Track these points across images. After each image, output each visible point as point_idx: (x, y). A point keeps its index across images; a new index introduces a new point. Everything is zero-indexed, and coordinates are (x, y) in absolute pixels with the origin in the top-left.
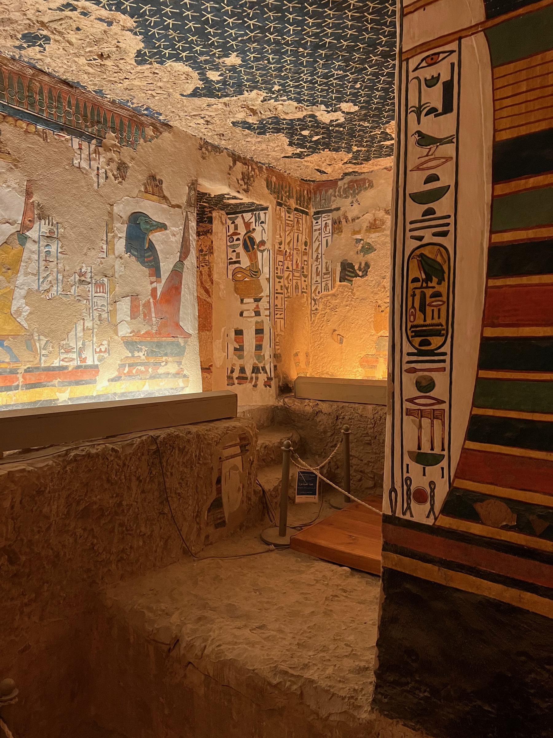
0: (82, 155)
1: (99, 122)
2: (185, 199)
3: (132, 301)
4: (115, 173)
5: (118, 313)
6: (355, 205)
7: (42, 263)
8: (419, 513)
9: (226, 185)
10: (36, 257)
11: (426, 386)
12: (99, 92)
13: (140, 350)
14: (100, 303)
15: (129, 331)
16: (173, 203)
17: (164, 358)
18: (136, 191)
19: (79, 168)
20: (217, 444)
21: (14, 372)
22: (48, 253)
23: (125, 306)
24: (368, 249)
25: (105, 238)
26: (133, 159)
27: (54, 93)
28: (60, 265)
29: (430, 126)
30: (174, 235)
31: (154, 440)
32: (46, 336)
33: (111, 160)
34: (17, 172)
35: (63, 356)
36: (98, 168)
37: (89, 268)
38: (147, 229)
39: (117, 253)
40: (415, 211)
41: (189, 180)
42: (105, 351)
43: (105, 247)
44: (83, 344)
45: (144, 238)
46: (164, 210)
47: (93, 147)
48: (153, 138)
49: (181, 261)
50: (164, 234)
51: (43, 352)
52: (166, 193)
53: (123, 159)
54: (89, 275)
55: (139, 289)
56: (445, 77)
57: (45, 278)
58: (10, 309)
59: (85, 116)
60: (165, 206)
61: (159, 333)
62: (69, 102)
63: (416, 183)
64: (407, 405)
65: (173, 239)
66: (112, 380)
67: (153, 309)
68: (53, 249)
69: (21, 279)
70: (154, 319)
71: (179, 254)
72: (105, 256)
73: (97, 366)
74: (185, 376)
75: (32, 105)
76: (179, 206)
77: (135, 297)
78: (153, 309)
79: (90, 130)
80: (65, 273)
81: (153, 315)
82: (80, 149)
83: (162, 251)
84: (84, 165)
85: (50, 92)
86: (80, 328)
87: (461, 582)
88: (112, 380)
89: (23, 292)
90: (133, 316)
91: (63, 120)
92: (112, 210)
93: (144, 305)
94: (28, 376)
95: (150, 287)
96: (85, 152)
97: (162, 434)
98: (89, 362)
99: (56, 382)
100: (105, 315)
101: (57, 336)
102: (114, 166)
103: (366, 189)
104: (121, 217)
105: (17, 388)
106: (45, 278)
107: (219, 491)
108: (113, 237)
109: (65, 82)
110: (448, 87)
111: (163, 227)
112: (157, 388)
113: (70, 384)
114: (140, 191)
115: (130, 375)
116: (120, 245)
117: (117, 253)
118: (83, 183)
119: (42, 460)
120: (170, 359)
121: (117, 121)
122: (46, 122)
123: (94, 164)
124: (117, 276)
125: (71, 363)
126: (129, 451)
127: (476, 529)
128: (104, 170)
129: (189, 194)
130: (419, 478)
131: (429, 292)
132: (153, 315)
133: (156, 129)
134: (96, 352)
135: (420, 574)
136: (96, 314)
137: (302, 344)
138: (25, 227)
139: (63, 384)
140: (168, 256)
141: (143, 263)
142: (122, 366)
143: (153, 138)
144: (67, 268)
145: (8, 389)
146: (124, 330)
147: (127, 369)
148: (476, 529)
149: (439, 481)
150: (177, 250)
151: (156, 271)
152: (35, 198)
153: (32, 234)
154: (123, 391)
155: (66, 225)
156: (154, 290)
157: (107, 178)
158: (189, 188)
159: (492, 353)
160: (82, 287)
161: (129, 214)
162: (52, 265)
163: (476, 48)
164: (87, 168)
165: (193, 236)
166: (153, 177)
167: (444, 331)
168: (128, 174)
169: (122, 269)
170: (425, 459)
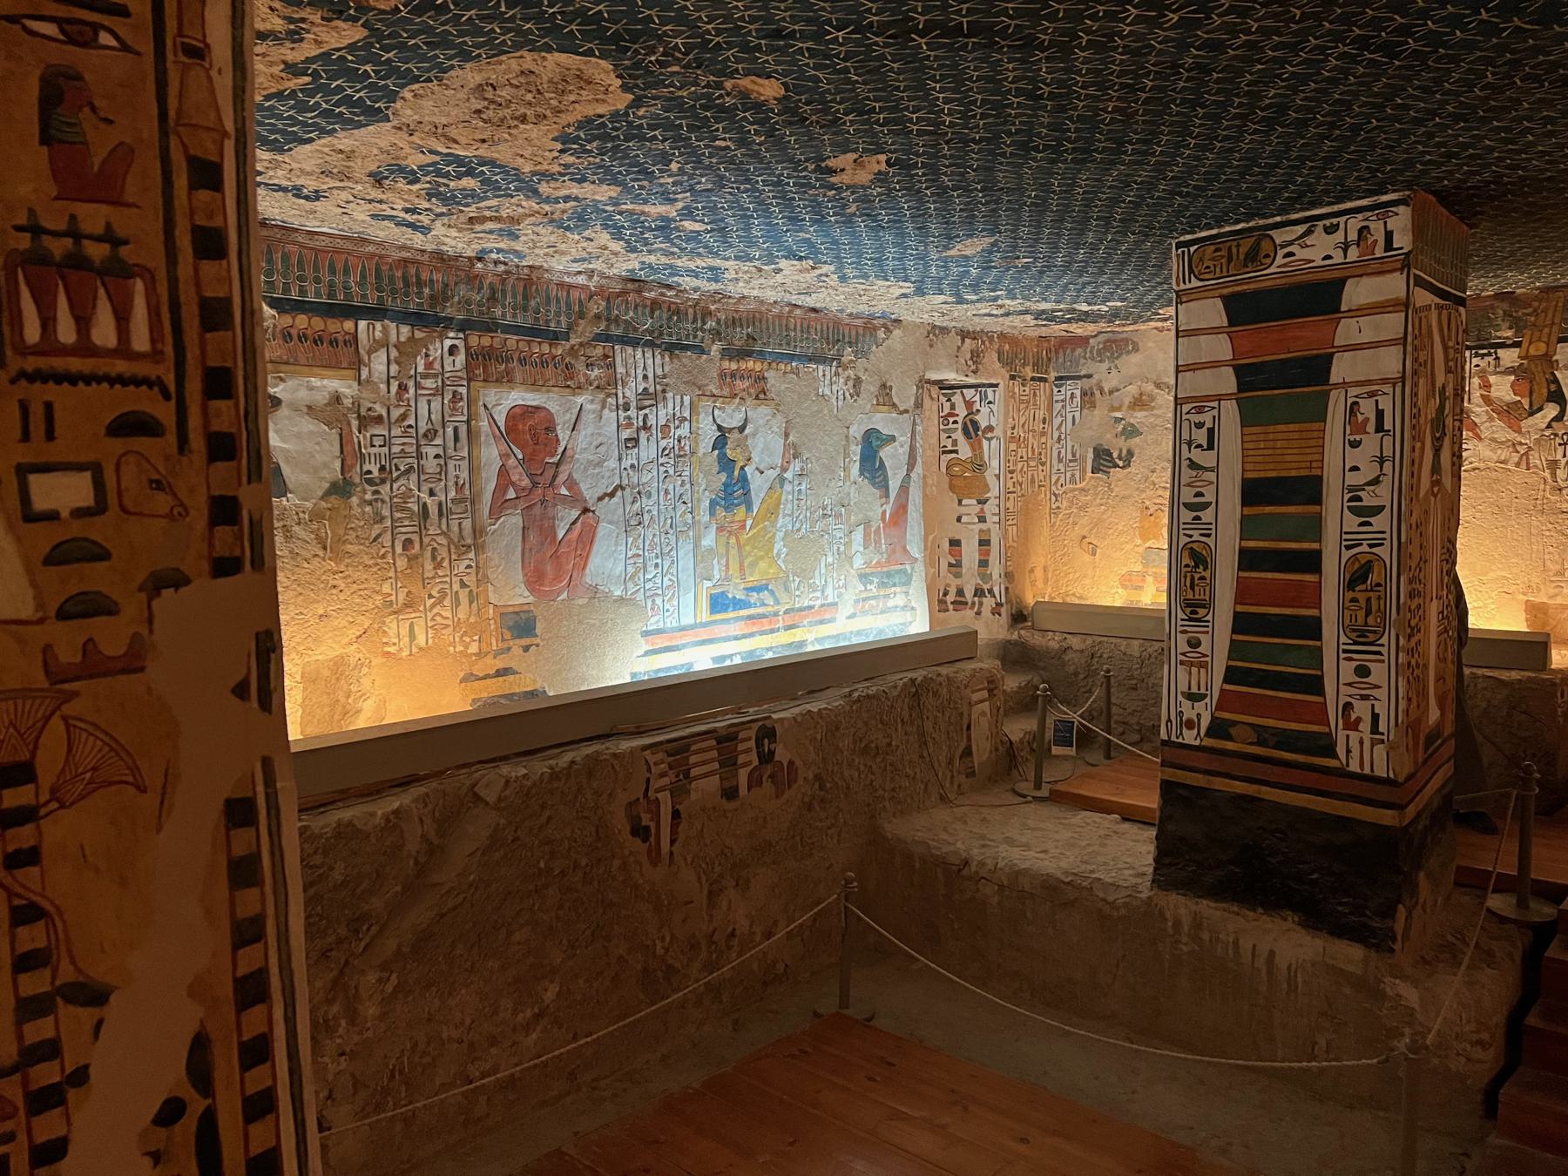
6: (1114, 372)
8: (1189, 737)
11: (1194, 644)
12: (842, 311)
20: (966, 686)
21: (776, 614)
24: (1131, 432)
29: (1196, 455)
31: (913, 681)
34: (779, 417)
40: (1187, 516)
41: (917, 377)
46: (893, 421)
49: (908, 475)
52: (896, 400)
56: (1209, 424)
61: (888, 561)
63: (1187, 495)
64: (1180, 657)
65: (901, 451)
66: (849, 617)
75: (788, 344)
76: (906, 411)
77: (867, 524)
84: (827, 392)
87: (1220, 784)
88: (849, 617)
97: (919, 675)
98: (830, 600)
101: (805, 574)
103: (1129, 352)
107: (969, 739)
110: (1211, 431)
115: (864, 613)
119: (827, 702)
122: (799, 358)
126: (895, 693)
127: (1230, 746)
131: (1197, 576)
133: (888, 330)
135: (1188, 782)
137: (1039, 559)
138: (784, 470)
145: (772, 631)
148: (1230, 746)
149: (1204, 713)
152: (791, 438)
153: (788, 475)
156: (884, 513)
159: (1241, 623)
163: (1230, 409)
166: (884, 386)
167: (1207, 605)
170: (1193, 697)
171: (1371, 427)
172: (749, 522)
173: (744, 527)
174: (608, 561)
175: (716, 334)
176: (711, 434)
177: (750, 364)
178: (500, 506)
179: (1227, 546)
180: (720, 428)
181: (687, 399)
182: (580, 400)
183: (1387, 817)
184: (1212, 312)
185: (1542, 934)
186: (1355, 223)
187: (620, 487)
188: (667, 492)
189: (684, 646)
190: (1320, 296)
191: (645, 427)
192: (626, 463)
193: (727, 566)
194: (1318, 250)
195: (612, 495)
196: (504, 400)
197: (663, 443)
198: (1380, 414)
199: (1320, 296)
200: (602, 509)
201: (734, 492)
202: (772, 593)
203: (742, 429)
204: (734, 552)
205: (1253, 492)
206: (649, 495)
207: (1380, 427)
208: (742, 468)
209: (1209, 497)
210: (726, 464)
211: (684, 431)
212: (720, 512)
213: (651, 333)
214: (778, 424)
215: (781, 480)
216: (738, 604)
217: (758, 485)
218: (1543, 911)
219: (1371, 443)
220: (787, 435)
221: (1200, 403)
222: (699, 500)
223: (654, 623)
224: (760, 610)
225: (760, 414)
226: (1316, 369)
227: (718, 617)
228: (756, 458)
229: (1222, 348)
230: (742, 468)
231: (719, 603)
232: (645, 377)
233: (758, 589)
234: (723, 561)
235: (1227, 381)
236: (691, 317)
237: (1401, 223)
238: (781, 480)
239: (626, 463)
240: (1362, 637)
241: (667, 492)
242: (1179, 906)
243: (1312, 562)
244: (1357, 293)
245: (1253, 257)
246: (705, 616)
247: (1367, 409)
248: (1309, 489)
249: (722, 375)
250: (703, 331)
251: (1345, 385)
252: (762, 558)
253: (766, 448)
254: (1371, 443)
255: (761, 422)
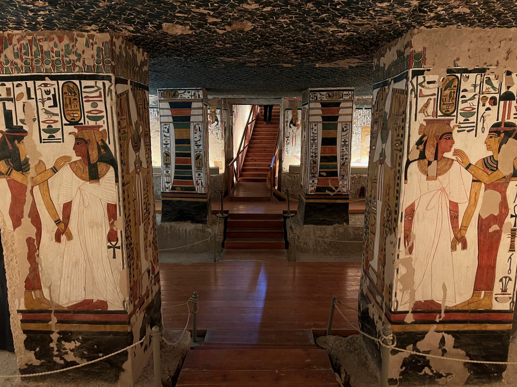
8: (167, 191)
11: (167, 172)
29: (165, 134)
40: (164, 146)
63: (164, 142)
87: (174, 199)
110: (168, 129)
127: (176, 191)
130: (167, 185)
148: (176, 191)
149: (170, 185)
159: (177, 167)
163: (172, 125)
167: (170, 164)
170: (168, 183)
171: (198, 130)
179: (173, 153)
183: (205, 200)
184: (167, 105)
185: (226, 218)
186: (193, 92)
190: (187, 105)
194: (186, 96)
198: (199, 128)
199: (187, 105)
205: (177, 142)
207: (200, 130)
209: (169, 142)
218: (225, 215)
219: (198, 133)
221: (166, 123)
226: (188, 119)
229: (169, 112)
235: (171, 120)
237: (201, 93)
240: (199, 168)
242: (167, 224)
243: (189, 155)
244: (194, 105)
245: (174, 95)
247: (197, 127)
248: (188, 141)
251: (193, 122)
254: (198, 133)
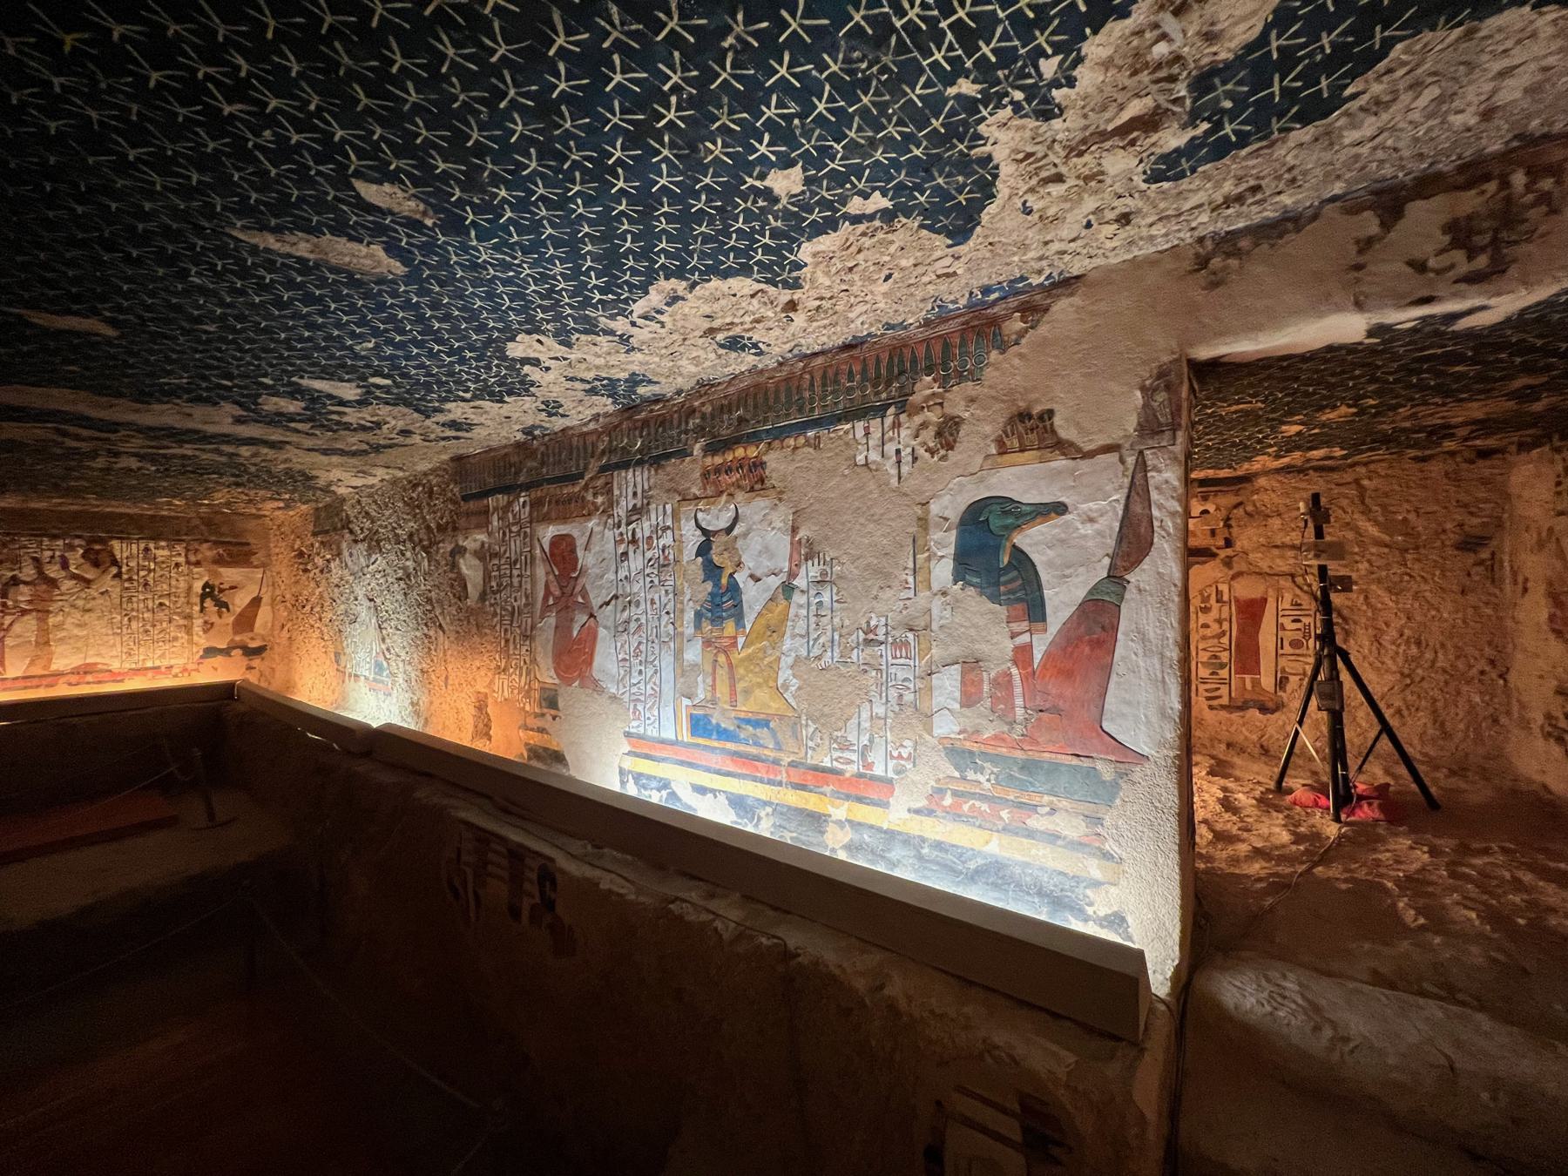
0: (871, 443)
1: (901, 373)
2: (1131, 423)
3: (963, 674)
4: (931, 445)
5: (935, 693)
7: (813, 619)
9: (1339, 309)
10: (804, 612)
13: (982, 770)
14: (901, 675)
15: (957, 729)
16: (1088, 447)
17: (1046, 798)
18: (979, 460)
19: (866, 465)
21: (776, 762)
22: (820, 603)
23: (948, 683)
25: (911, 565)
26: (973, 400)
27: (830, 373)
28: (836, 620)
30: (1091, 520)
32: (814, 722)
33: (924, 425)
34: (782, 508)
35: (836, 754)
36: (898, 452)
37: (883, 620)
38: (1006, 527)
39: (936, 587)
41: (1146, 373)
42: (909, 758)
43: (911, 579)
44: (871, 741)
45: (997, 549)
47: (889, 420)
48: (1022, 334)
49: (1116, 578)
50: (1056, 526)
51: (811, 744)
52: (1063, 434)
53: (948, 410)
54: (881, 631)
55: (983, 648)
57: (816, 640)
58: (776, 681)
59: (878, 376)
60: (1061, 463)
62: (851, 372)
65: (1088, 530)
66: (917, 812)
67: (1018, 690)
68: (826, 598)
69: (787, 643)
70: (1020, 712)
71: (1107, 561)
72: (911, 594)
73: (890, 782)
74: (1107, 856)
75: (800, 410)
77: (971, 665)
78: (1018, 690)
79: (884, 396)
80: (844, 631)
81: (1019, 701)
82: (867, 434)
83: (1050, 564)
84: (874, 456)
85: (824, 377)
86: (865, 715)
88: (917, 812)
89: (790, 660)
90: (968, 700)
91: (841, 406)
92: (928, 512)
93: (995, 683)
94: (792, 770)
95: (1009, 645)
96: (876, 435)
98: (878, 770)
99: (827, 789)
100: (908, 697)
102: (928, 435)
104: (946, 519)
105: (780, 784)
106: (816, 640)
108: (929, 559)
109: (847, 347)
111: (1060, 509)
112: (1018, 857)
113: (848, 797)
114: (987, 457)
115: (956, 815)
116: (943, 571)
117: (936, 587)
118: (872, 486)
120: (1064, 803)
121: (937, 349)
122: (816, 423)
123: (890, 448)
124: (935, 626)
125: (848, 767)
128: (909, 450)
129: (1146, 406)
132: (1019, 701)
134: (892, 757)
136: (893, 693)
138: (792, 575)
139: (837, 795)
140: (1067, 572)
141: (995, 598)
142: (940, 792)
143: (1022, 334)
144: (847, 622)
146: (946, 726)
147: (948, 801)
150: (1101, 552)
151: (1035, 611)
153: (800, 582)
154: (938, 838)
155: (844, 559)
157: (915, 459)
158: (1143, 389)
160: (869, 650)
161: (963, 507)
162: (825, 620)
164: (879, 458)
165: (1165, 506)
168: (962, 433)
169: (947, 613)
172: (741, 640)
173: (735, 644)
174: (607, 658)
175: (700, 431)
176: (693, 539)
177: (740, 452)
178: (546, 608)
180: (705, 532)
181: (668, 507)
182: (590, 525)
187: (616, 597)
188: (653, 602)
189: (664, 760)
191: (634, 541)
192: (622, 574)
193: (713, 686)
195: (607, 604)
196: (549, 532)
197: (649, 555)
200: (599, 615)
201: (723, 602)
202: (773, 733)
203: (729, 530)
204: (722, 673)
206: (638, 604)
208: (731, 575)
210: (712, 570)
211: (667, 540)
212: (707, 626)
213: (640, 451)
214: (781, 517)
215: (788, 589)
216: (724, 734)
217: (753, 596)
220: (794, 530)
222: (682, 611)
223: (635, 727)
224: (753, 750)
225: (755, 509)
227: (700, 741)
228: (749, 561)
230: (731, 575)
231: (699, 725)
232: (635, 494)
233: (757, 724)
234: (709, 680)
236: (675, 422)
238: (788, 589)
239: (622, 574)
241: (653, 602)
246: (686, 737)
249: (705, 475)
250: (686, 432)
252: (759, 685)
253: (766, 550)
255: (757, 518)
